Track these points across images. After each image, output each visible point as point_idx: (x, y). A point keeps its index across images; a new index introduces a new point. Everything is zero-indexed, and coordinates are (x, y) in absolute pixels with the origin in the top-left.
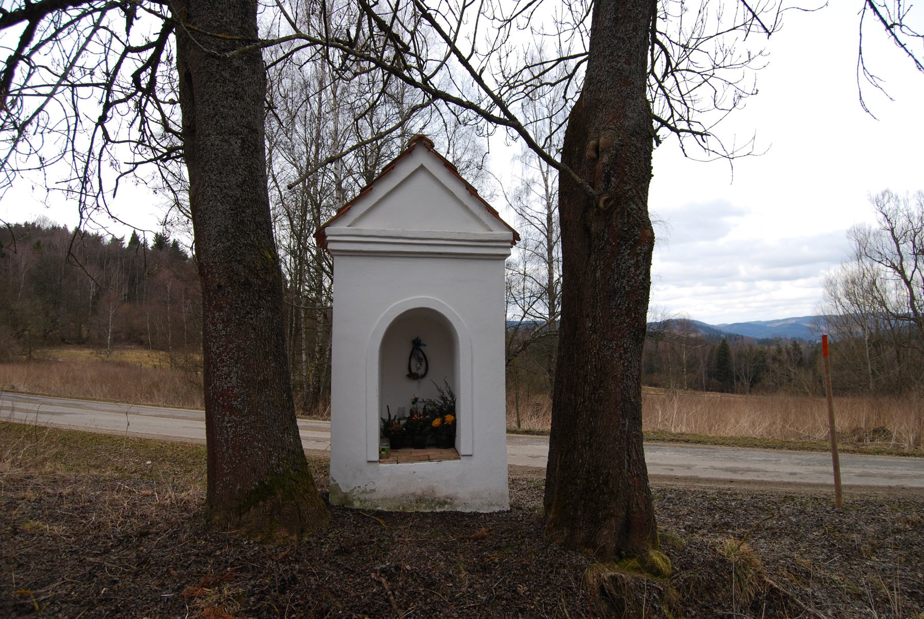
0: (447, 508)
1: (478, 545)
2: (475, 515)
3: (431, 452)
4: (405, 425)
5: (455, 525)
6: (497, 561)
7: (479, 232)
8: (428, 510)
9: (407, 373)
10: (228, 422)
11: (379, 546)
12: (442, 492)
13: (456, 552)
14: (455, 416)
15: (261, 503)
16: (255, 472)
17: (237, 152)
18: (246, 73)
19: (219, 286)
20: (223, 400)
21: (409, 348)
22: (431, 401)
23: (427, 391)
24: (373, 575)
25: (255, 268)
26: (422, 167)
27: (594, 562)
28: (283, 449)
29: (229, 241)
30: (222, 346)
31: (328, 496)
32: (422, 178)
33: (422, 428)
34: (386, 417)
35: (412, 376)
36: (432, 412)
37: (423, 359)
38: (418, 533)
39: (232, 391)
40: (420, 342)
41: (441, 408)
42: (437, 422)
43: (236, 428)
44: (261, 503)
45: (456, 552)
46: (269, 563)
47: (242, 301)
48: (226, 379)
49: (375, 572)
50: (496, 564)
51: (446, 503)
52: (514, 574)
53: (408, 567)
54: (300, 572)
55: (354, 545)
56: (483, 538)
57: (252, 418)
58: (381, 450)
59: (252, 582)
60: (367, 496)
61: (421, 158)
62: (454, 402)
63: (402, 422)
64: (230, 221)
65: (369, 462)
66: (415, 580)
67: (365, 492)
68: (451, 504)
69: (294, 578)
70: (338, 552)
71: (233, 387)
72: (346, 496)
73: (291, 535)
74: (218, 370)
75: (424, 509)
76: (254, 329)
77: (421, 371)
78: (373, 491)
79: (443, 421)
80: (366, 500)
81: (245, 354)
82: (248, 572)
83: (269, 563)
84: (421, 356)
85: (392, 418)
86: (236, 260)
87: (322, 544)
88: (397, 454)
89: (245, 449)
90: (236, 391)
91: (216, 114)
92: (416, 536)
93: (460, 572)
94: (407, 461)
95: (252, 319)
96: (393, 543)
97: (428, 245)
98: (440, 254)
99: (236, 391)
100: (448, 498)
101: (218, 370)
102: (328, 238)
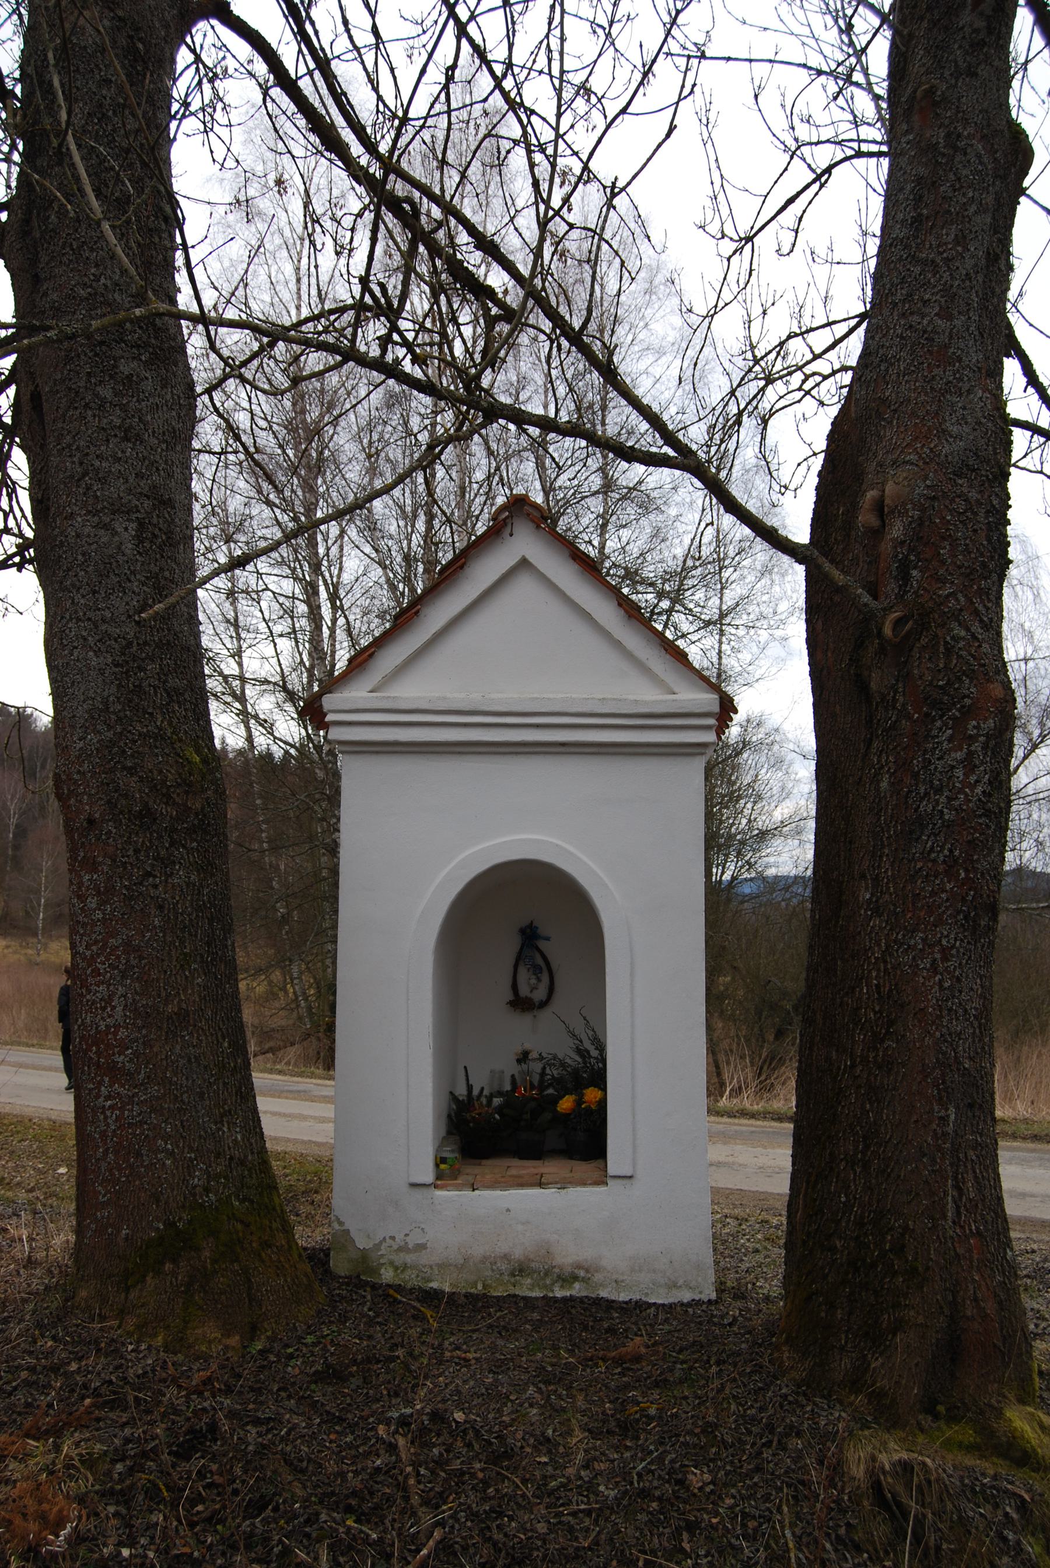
0: (577, 1290)
1: (622, 1374)
2: (636, 1309)
3: (550, 1168)
4: (500, 1110)
5: (585, 1328)
6: (652, 1411)
7: (645, 695)
8: (537, 1293)
9: (511, 997)
10: (108, 1098)
11: (406, 1366)
12: (568, 1254)
13: (569, 1388)
14: (604, 1090)
15: (168, 1266)
17: (128, 547)
18: (148, 386)
19: (91, 821)
20: (99, 1054)
21: (511, 945)
22: (555, 1057)
23: (547, 1037)
24: (381, 1430)
25: (164, 782)
26: (524, 563)
27: (866, 1426)
28: (218, 1155)
29: (110, 727)
30: (96, 942)
31: (327, 1255)
32: (524, 587)
33: (534, 1117)
34: (461, 1091)
35: (521, 1004)
36: (557, 1082)
37: (545, 968)
38: (500, 1342)
39: (115, 1034)
40: (525, 933)
41: (576, 1073)
42: (566, 1104)
43: (122, 1109)
44: (168, 1266)
45: (569, 1388)
46: (171, 1393)
47: (137, 851)
48: (104, 1009)
49: (388, 1422)
50: (650, 1419)
51: (575, 1278)
52: (686, 1444)
53: (459, 1416)
54: (231, 1415)
55: (354, 1362)
56: (637, 1359)
57: (154, 1090)
58: (439, 1161)
59: (127, 1431)
60: (410, 1258)
62: (604, 1061)
63: (497, 1101)
64: (114, 689)
65: (414, 1185)
66: (469, 1445)
67: (403, 1249)
68: (585, 1280)
69: (213, 1427)
70: (318, 1378)
71: (117, 1027)
72: (364, 1256)
73: (227, 1334)
74: (89, 991)
75: (527, 1289)
76: (161, 907)
78: (421, 1247)
80: (405, 1267)
81: (141, 958)
82: (124, 1410)
83: (171, 1393)
84: (540, 961)
85: (476, 1092)
86: (124, 768)
87: (291, 1357)
88: (477, 1170)
89: (138, 1155)
90: (122, 1033)
91: (85, 474)
92: (493, 1348)
93: (570, 1433)
94: (492, 1186)
95: (155, 886)
96: (440, 1363)
98: (563, 744)
99: (122, 1033)
100: (579, 1267)
101: (89, 991)
102: (329, 718)
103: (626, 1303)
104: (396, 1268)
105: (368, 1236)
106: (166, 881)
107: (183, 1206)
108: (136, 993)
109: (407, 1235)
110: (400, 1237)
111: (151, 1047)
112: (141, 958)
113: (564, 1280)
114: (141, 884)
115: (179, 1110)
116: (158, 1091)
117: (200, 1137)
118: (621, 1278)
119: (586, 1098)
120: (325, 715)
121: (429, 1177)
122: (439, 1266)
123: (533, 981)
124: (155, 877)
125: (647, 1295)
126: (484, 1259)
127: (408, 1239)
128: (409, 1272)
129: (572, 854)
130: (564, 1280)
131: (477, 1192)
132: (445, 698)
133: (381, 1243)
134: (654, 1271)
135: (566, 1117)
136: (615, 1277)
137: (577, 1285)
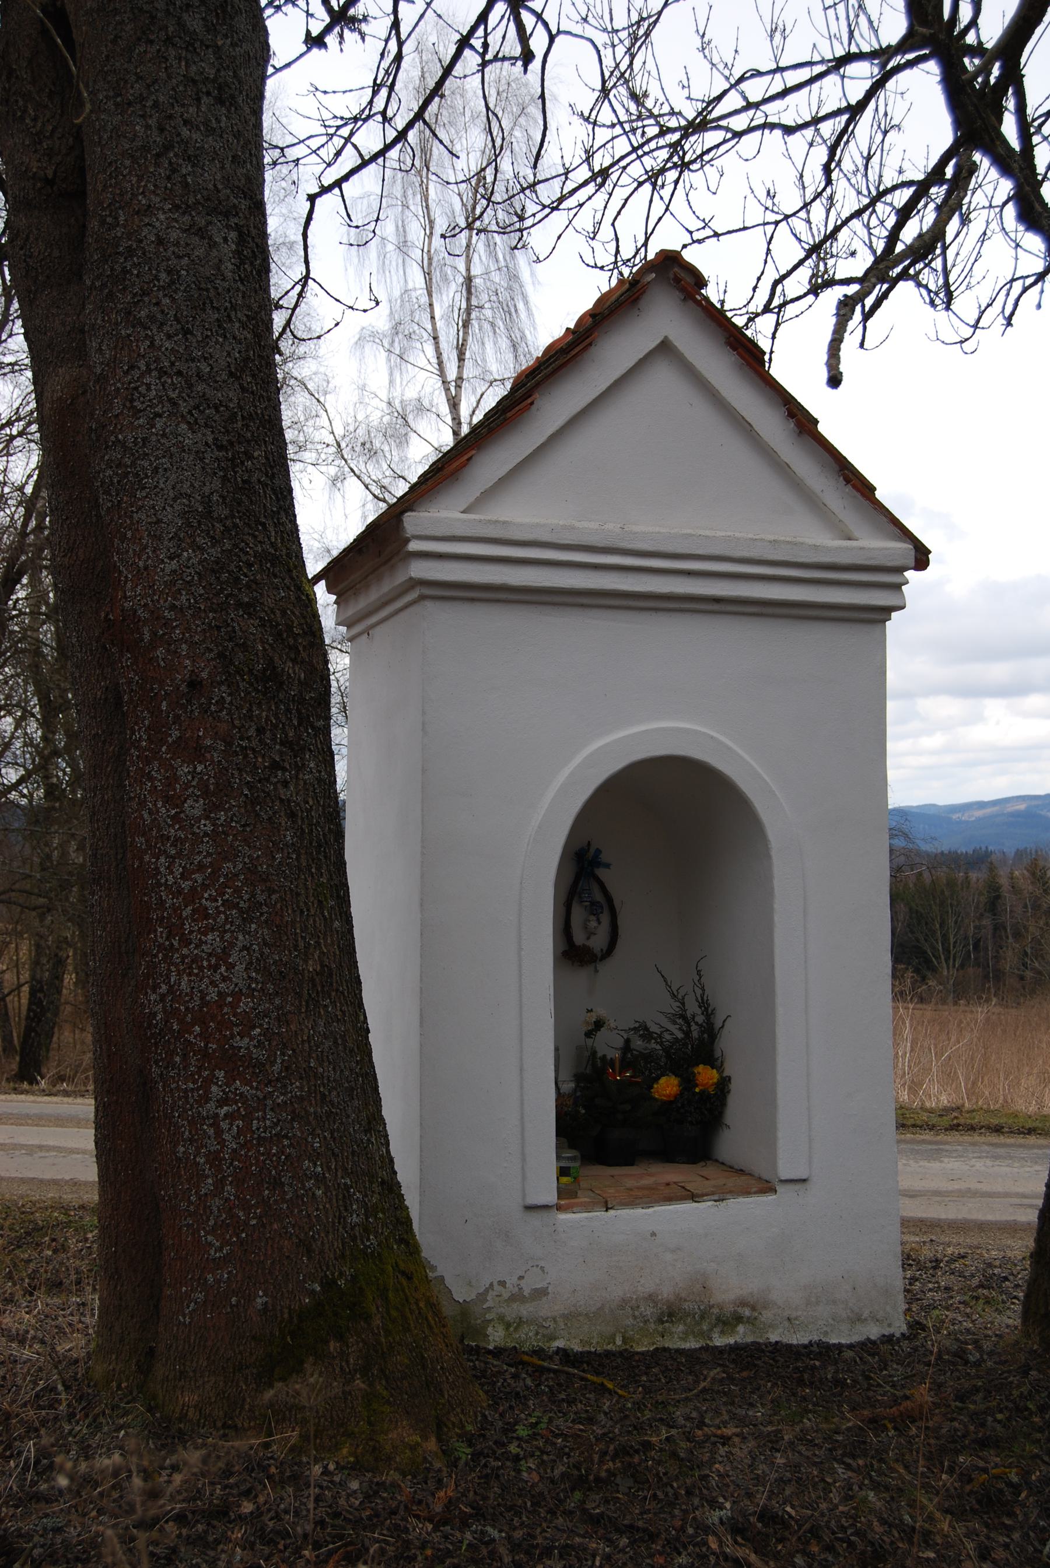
0: (741, 1335)
7: (815, 539)
8: (692, 1344)
10: (222, 1102)
12: (730, 1287)
15: (333, 1346)
16: (309, 1251)
17: (228, 267)
19: (194, 684)
20: (204, 1036)
25: (289, 628)
26: (665, 348)
29: (215, 542)
30: (201, 867)
33: (647, 1106)
37: (607, 906)
39: (234, 1006)
40: (651, 852)
42: (667, 1086)
43: (248, 1118)
44: (333, 1346)
47: (260, 731)
48: (215, 968)
50: (1016, 1489)
51: (739, 1319)
60: (525, 1310)
61: (663, 320)
64: (217, 484)
65: (530, 1208)
67: (517, 1297)
68: (751, 1321)
71: (237, 995)
73: (425, 1438)
74: (186, 942)
75: (681, 1339)
76: (292, 815)
77: (598, 942)
78: (541, 1293)
79: (688, 1082)
80: (520, 1322)
81: (271, 891)
84: (599, 897)
86: (239, 604)
89: (276, 1184)
90: (245, 1005)
91: (168, 147)
95: (286, 784)
97: (689, 573)
98: (717, 600)
99: (245, 1005)
100: (743, 1304)
101: (186, 942)
102: (414, 546)
103: (805, 1346)
104: (508, 1325)
105: (470, 1284)
106: (297, 778)
107: (343, 1256)
108: (265, 944)
109: (521, 1278)
110: (511, 1281)
111: (288, 1023)
112: (271, 891)
113: (725, 1323)
114: (268, 780)
115: (329, 1114)
116: (301, 1089)
117: (353, 1153)
118: (794, 1315)
119: (700, 1079)
120: (407, 541)
121: (550, 1197)
122: (566, 1317)
123: (593, 924)
124: (284, 769)
125: (826, 1333)
126: (624, 1302)
127: (523, 1283)
128: (525, 1329)
129: (729, 748)
130: (725, 1323)
131: (612, 1212)
132: (573, 528)
133: (487, 1291)
134: (834, 1302)
135: (668, 1106)
136: (786, 1314)
137: (741, 1328)
